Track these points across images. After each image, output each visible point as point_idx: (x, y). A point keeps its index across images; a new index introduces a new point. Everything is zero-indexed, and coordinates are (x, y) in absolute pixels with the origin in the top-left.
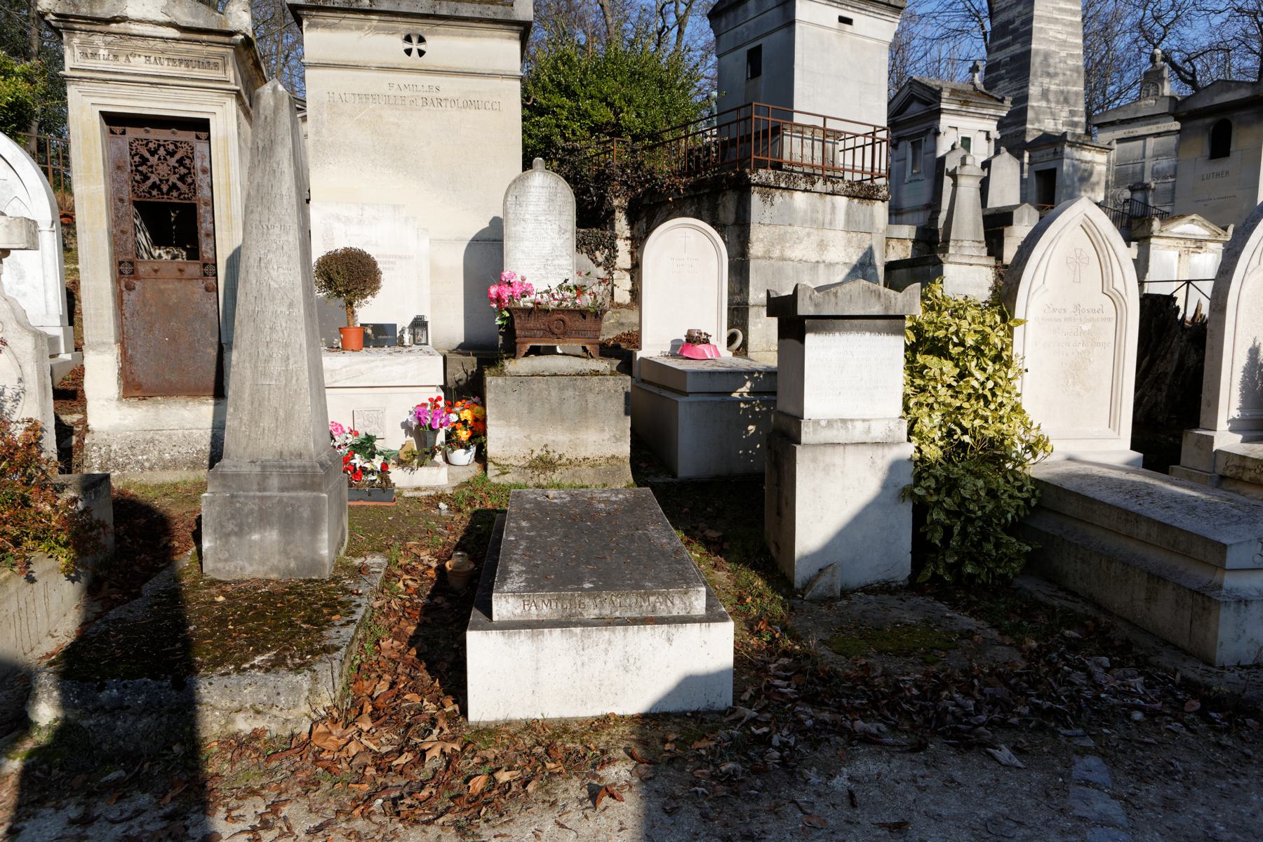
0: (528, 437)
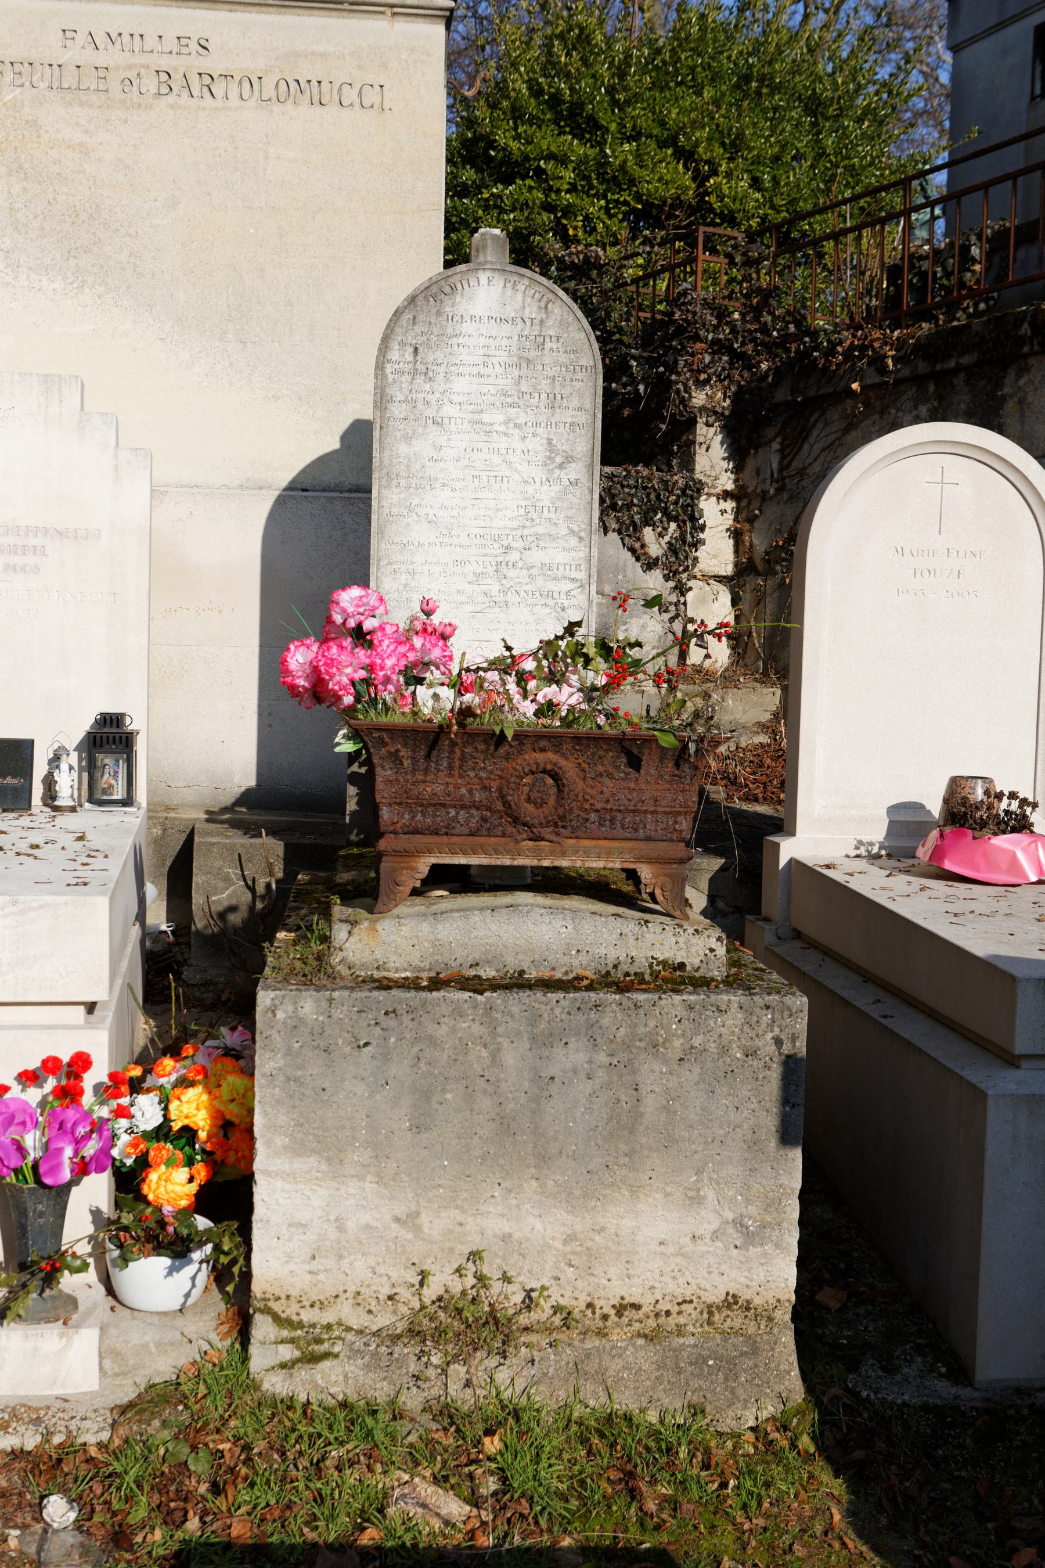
0: (409, 1220)
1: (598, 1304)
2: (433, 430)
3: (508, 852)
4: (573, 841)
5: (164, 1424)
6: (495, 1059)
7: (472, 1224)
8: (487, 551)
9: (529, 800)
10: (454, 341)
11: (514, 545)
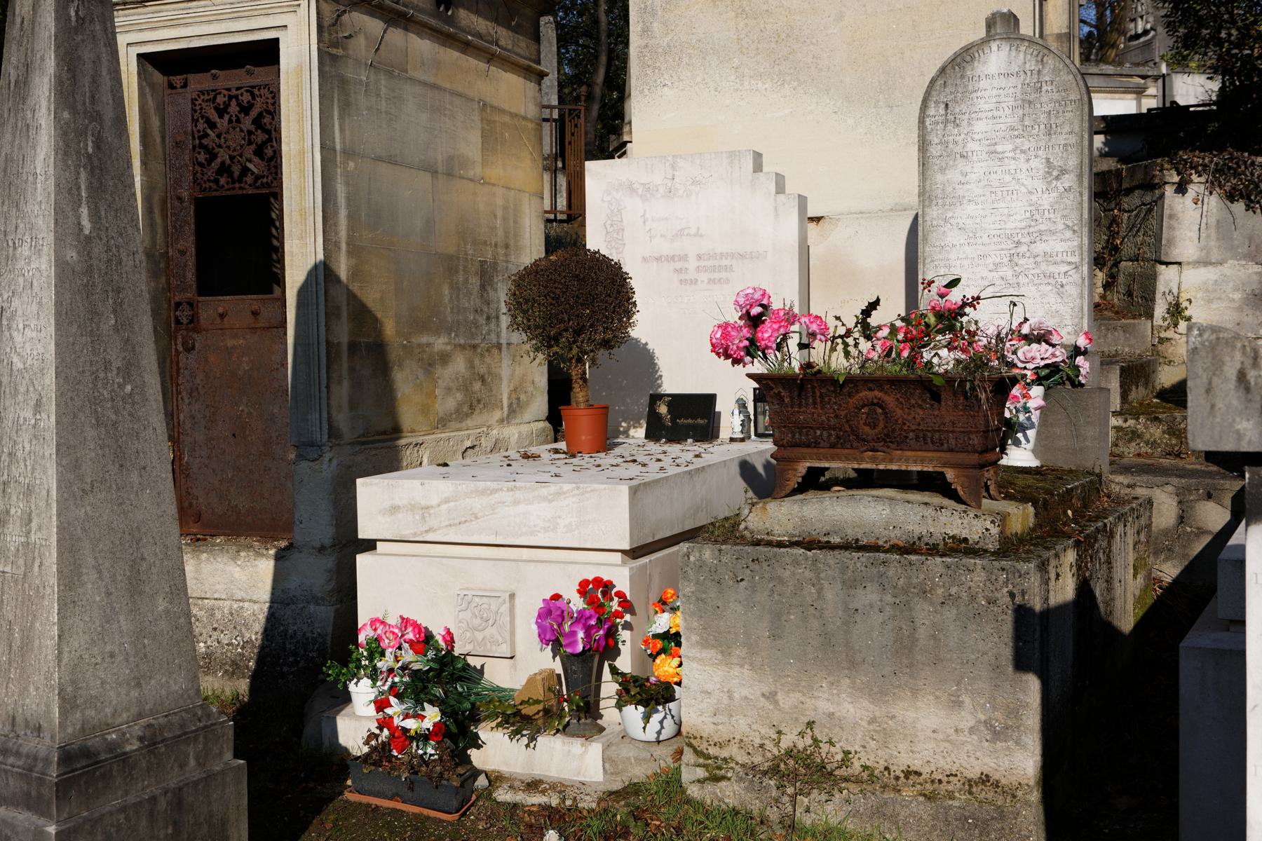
0: (771, 696)
1: (892, 768)
2: (961, 163)
3: (855, 459)
4: (899, 452)
5: (628, 805)
6: (820, 595)
7: (809, 703)
8: (1003, 246)
9: (865, 424)
10: (974, 95)
11: (1023, 240)
